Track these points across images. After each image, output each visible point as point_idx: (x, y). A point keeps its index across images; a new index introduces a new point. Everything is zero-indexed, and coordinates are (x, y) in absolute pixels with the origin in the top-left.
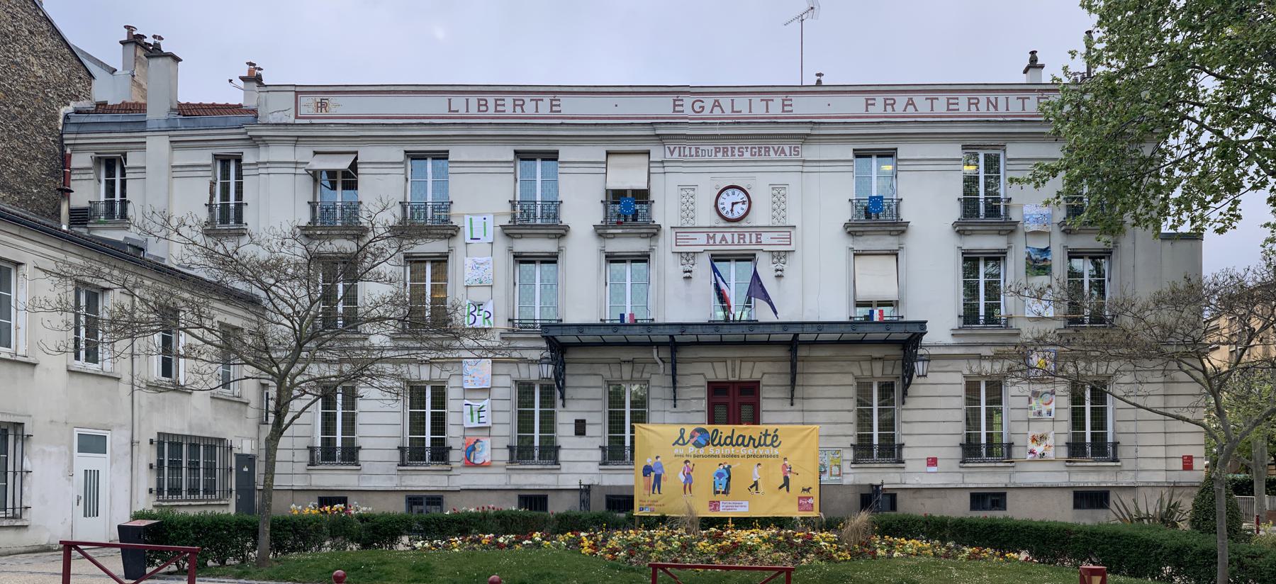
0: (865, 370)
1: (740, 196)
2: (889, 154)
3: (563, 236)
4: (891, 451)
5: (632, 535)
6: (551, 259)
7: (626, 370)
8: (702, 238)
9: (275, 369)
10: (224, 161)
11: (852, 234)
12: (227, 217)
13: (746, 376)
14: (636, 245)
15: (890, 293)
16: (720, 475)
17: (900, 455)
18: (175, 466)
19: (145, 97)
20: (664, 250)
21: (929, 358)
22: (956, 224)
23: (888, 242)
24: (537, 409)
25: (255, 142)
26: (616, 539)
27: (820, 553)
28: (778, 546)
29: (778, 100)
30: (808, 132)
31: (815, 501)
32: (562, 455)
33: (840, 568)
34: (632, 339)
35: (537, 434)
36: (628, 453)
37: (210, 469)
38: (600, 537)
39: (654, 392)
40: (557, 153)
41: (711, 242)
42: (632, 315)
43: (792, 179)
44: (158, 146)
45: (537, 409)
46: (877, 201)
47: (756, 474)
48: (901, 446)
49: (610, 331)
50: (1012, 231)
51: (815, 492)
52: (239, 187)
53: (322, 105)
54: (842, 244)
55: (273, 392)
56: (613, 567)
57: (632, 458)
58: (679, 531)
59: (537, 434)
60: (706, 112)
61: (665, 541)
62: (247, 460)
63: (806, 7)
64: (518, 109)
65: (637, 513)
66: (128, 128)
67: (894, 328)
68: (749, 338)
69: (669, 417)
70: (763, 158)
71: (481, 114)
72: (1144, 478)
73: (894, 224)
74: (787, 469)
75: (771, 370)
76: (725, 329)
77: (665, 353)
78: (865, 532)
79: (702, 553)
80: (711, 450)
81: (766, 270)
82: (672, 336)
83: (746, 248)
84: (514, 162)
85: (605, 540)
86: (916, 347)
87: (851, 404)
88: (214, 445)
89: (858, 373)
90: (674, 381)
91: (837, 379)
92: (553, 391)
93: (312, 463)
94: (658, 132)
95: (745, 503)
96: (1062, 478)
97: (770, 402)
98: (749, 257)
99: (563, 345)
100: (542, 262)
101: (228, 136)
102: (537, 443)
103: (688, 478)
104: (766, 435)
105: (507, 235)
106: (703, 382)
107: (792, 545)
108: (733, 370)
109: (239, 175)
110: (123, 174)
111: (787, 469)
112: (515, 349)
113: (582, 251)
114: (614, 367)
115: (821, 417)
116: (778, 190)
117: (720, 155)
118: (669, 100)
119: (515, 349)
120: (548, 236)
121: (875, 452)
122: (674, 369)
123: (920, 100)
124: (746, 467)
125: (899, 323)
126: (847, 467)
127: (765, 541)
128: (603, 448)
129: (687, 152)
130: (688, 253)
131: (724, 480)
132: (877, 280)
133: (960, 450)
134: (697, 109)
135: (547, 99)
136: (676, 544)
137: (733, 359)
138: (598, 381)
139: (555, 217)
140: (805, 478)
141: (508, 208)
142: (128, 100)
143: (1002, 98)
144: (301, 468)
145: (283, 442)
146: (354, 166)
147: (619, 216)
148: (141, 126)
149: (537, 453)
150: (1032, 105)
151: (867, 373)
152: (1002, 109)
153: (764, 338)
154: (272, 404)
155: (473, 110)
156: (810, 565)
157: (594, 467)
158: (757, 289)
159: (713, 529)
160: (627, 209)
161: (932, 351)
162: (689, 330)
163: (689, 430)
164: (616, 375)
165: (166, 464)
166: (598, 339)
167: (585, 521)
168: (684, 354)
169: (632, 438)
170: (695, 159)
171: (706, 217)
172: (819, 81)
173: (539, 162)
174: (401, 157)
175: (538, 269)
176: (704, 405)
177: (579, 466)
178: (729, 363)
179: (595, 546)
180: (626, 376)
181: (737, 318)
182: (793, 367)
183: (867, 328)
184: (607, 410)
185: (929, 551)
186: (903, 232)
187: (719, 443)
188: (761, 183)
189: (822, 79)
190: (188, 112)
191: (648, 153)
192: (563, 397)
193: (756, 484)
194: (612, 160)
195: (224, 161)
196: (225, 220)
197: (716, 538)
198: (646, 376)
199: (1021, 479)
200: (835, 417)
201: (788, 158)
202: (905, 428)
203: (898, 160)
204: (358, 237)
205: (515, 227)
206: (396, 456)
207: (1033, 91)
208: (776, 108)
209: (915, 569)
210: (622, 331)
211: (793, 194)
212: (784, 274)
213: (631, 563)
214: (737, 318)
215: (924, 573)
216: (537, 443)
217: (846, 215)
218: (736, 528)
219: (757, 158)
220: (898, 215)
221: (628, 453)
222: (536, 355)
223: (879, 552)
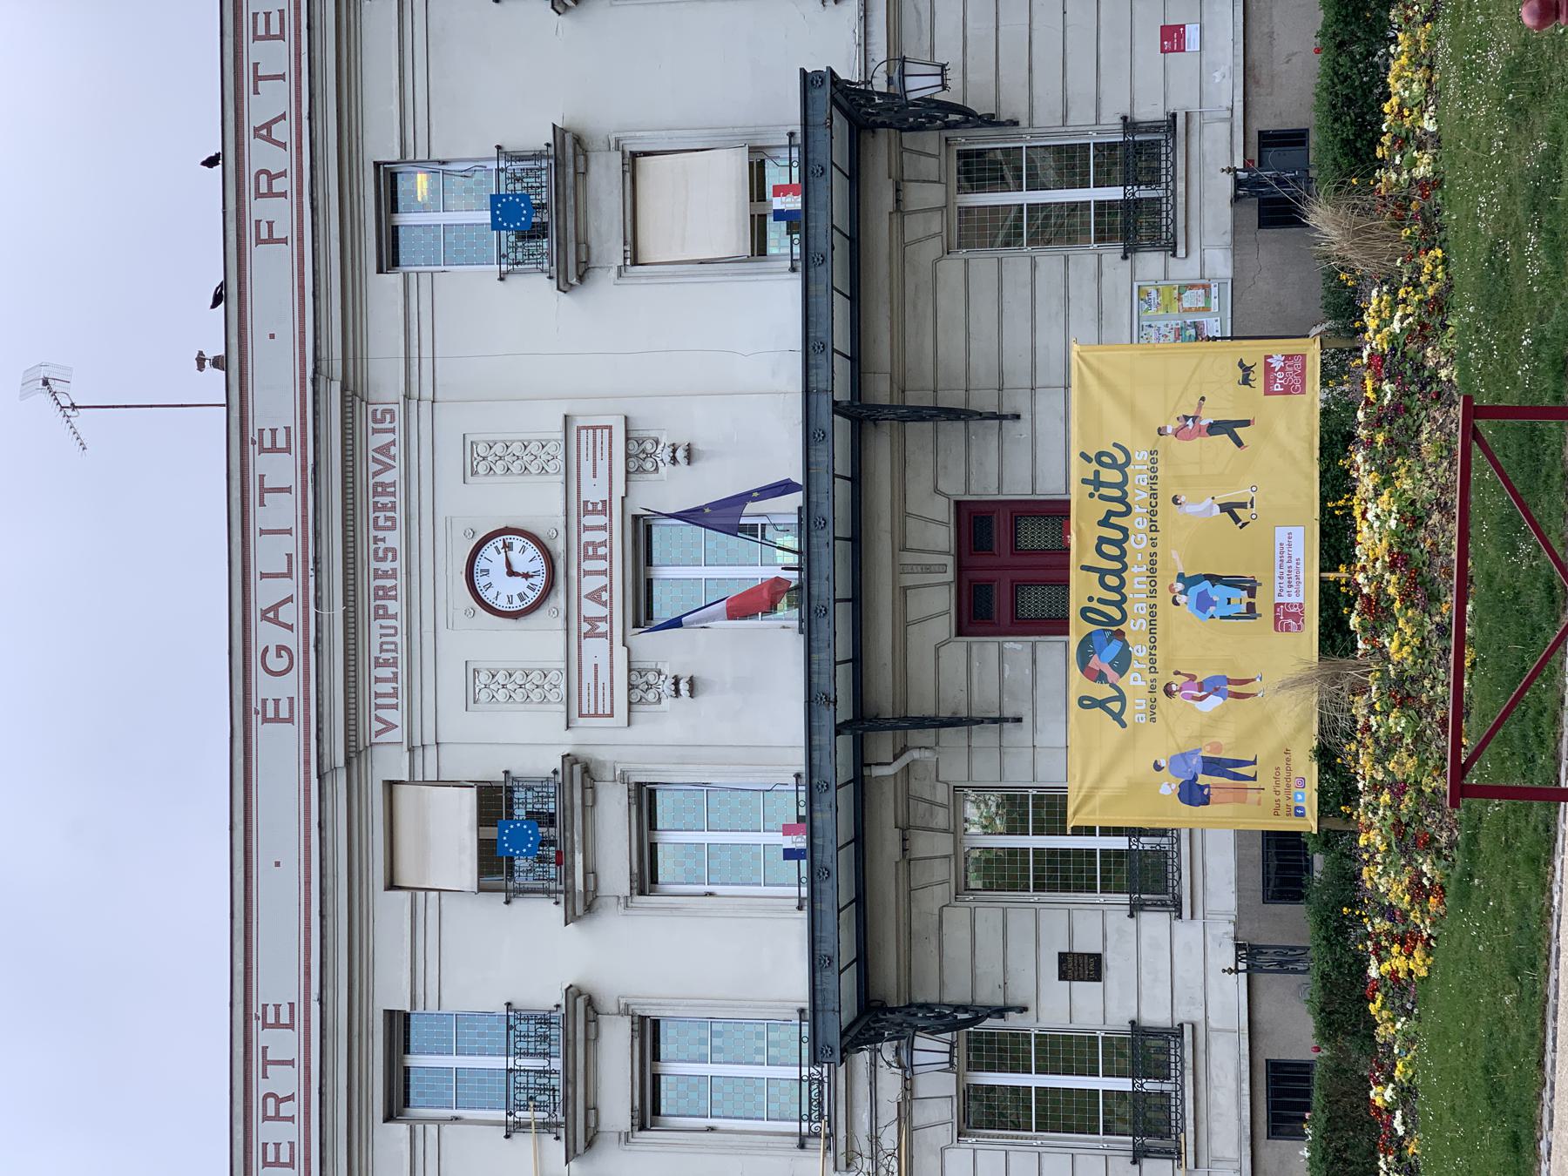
0: (927, 228)
1: (492, 557)
2: (389, 179)
3: (590, 1002)
4: (1142, 152)
5: (1373, 838)
6: (648, 1033)
7: (924, 844)
8: (595, 650)
13: (941, 537)
14: (614, 812)
15: (731, 167)
16: (1203, 603)
17: (1153, 127)
23: (605, 177)
24: (1033, 1080)
26: (1385, 882)
27: (1422, 332)
28: (1405, 445)
29: (262, 464)
30: (336, 387)
31: (1277, 350)
32: (1156, 1016)
33: (1466, 274)
34: (846, 831)
35: (1100, 1083)
36: (1146, 842)
38: (1381, 925)
39: (985, 772)
40: (390, 1015)
41: (603, 627)
42: (787, 830)
43: (453, 425)
45: (1033, 1080)
46: (503, 210)
47: (1202, 507)
48: (1129, 124)
49: (826, 887)
51: (1253, 351)
56: (1464, 895)
57: (1162, 833)
58: (1360, 711)
59: (1100, 1083)
60: (291, 640)
61: (1388, 751)
63: (44, 397)
64: (287, 1109)
65: (1310, 824)
67: (820, 156)
68: (843, 529)
69: (1050, 734)
70: (400, 501)
73: (559, 164)
74: (1189, 427)
75: (927, 473)
76: (821, 589)
77: (882, 744)
78: (1365, 212)
79: (1422, 650)
80: (1135, 628)
81: (671, 490)
82: (839, 729)
84: (412, 1123)
85: (1389, 912)
86: (868, 95)
87: (1017, 261)
89: (934, 247)
90: (954, 722)
91: (950, 303)
92: (982, 1034)
94: (340, 760)
95: (1281, 534)
97: (1007, 471)
98: (642, 531)
100: (656, 1057)
102: (1125, 1084)
103: (1213, 686)
104: (1097, 483)
105: (589, 1144)
107: (1398, 409)
108: (927, 569)
111: (1189, 427)
112: (874, 1139)
114: (919, 878)
115: (1049, 337)
116: (479, 460)
117: (393, 607)
118: (264, 734)
119: (874, 1139)
120: (592, 1040)
121: (1144, 193)
122: (922, 723)
124: (1186, 536)
125: (806, 141)
126: (1184, 269)
127: (1387, 482)
128: (1135, 909)
129: (386, 688)
130: (631, 687)
131: (1218, 593)
132: (698, 204)
134: (282, 663)
135: (262, 1037)
136: (1397, 722)
137: (899, 569)
138: (957, 918)
139: (545, 1021)
140: (1211, 377)
141: (524, 1143)
147: (542, 859)
149: (1150, 1086)
153: (843, 489)
156: (1458, 357)
157: (1188, 932)
158: (723, 517)
159: (1354, 621)
160: (524, 837)
161: (879, 52)
162: (823, 682)
163: (1079, 684)
164: (941, 870)
166: (848, 916)
167: (1338, 965)
168: (883, 697)
169: (1106, 831)
170: (402, 669)
171: (541, 641)
172: (216, 363)
173: (414, 1061)
175: (673, 1068)
176: (1016, 646)
177: (1183, 971)
178: (908, 580)
179: (1407, 941)
180: (944, 844)
181: (793, 559)
183: (820, 224)
184: (1032, 896)
185: (1421, 35)
186: (578, 140)
187: (1119, 605)
188: (464, 505)
189: (209, 355)
191: (390, 785)
192: (1001, 1012)
193: (1228, 508)
194: (406, 877)
197: (1379, 612)
198: (942, 794)
200: (1049, 304)
201: (399, 437)
202: (1081, 116)
203: (403, 160)
205: (569, 1125)
208: (279, 469)
209: (1470, 71)
210: (826, 856)
211: (490, 423)
212: (682, 441)
213: (1452, 845)
214: (793, 559)
215: (1483, 45)
216: (1125, 1084)
217: (536, 288)
218: (1351, 559)
219: (399, 515)
220: (537, 156)
221: (1146, 842)
222: (891, 1084)
223: (1421, 171)
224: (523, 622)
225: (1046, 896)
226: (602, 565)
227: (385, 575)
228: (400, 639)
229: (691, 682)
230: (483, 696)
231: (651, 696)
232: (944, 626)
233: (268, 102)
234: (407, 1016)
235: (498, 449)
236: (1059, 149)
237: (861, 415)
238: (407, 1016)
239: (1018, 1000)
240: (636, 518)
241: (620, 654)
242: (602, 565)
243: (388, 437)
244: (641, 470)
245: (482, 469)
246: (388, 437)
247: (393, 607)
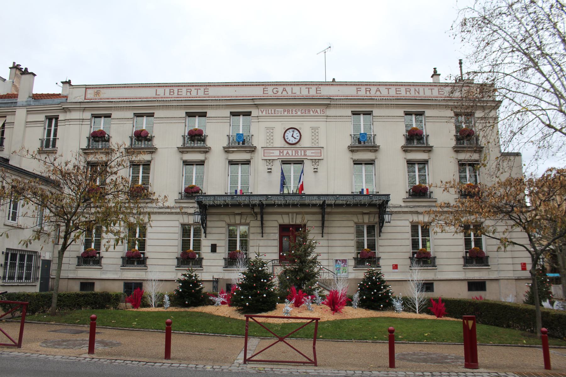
0: (359, 219)
6: (201, 163)
7: (238, 218)
8: (277, 153)
9: (66, 217)
10: (50, 119)
11: (352, 151)
12: (49, 145)
18: (13, 266)
19: (17, 91)
20: (258, 160)
21: (391, 213)
22: (403, 147)
24: (192, 239)
25: (65, 110)
29: (314, 88)
30: (329, 103)
32: (204, 263)
37: (29, 267)
39: (252, 230)
40: (206, 113)
42: (241, 191)
43: (322, 125)
44: (21, 114)
45: (192, 239)
48: (379, 258)
49: (230, 198)
50: (430, 151)
52: (56, 131)
53: (97, 93)
54: (347, 158)
55: (63, 228)
60: (279, 94)
62: (47, 263)
64: (189, 93)
66: (9, 105)
70: (307, 115)
71: (170, 96)
72: (503, 275)
73: (373, 147)
75: (311, 219)
83: (299, 156)
86: (385, 208)
87: (353, 236)
88: (32, 255)
89: (356, 220)
90: (262, 224)
93: (78, 265)
94: (256, 103)
96: (461, 276)
98: (301, 162)
99: (209, 208)
100: (197, 165)
101: (53, 109)
106: (277, 225)
108: (293, 219)
109: (56, 125)
113: (217, 161)
115: (338, 243)
116: (315, 130)
117: (286, 113)
120: (200, 152)
123: (382, 89)
129: (270, 112)
130: (270, 160)
133: (409, 261)
134: (275, 92)
135: (202, 89)
137: (293, 213)
142: (10, 93)
143: (421, 89)
144: (73, 267)
145: (66, 254)
150: (435, 92)
151: (361, 221)
152: (422, 94)
154: (62, 234)
155: (167, 94)
157: (221, 269)
164: (233, 221)
165: (9, 264)
171: (279, 142)
174: (132, 116)
176: (277, 236)
178: (290, 215)
182: (323, 217)
183: (362, 198)
184: (227, 239)
188: (306, 127)
190: (37, 97)
192: (205, 232)
195: (50, 119)
196: (47, 146)
198: (248, 221)
199: (440, 276)
200: (344, 243)
201: (319, 114)
202: (381, 249)
204: (107, 154)
206: (120, 262)
207: (436, 86)
208: (313, 92)
212: (318, 170)
217: (349, 142)
220: (374, 142)
222: (192, 211)
225: (227, 242)
226: (294, 154)
227: (292, 112)
228: (279, 115)
229: (270, 172)
230: (268, 131)
231: (268, 164)
232: (281, 222)
234: (205, 116)
235: (317, 134)
236: (375, 245)
237: (323, 206)
238: (205, 116)
239: (207, 236)
240: (303, 161)
241: (276, 158)
242: (294, 154)
243: (319, 112)
244: (313, 162)
246: (319, 112)
247: (286, 113)
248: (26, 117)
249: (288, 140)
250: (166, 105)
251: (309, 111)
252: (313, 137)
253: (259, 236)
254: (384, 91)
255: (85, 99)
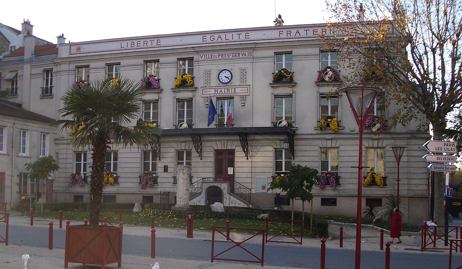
7: (183, 144)
8: (213, 91)
13: (229, 148)
25: (57, 64)
43: (248, 66)
53: (79, 49)
60: (215, 40)
108: (224, 145)
109: (52, 76)
110: (52, 76)
114: (178, 144)
117: (220, 57)
129: (208, 57)
135: (156, 40)
146: (16, 76)
148: (22, 61)
155: (129, 47)
171: (214, 82)
178: (223, 142)
217: (270, 79)
224: (217, 79)
232: (216, 148)
233: (303, 32)
239: (161, 159)
245: (242, 71)
248: (31, 71)
249: (221, 80)
250: (127, 56)
251: (239, 54)
252: (242, 77)
253: (199, 159)
254: (303, 32)
255: (70, 54)
